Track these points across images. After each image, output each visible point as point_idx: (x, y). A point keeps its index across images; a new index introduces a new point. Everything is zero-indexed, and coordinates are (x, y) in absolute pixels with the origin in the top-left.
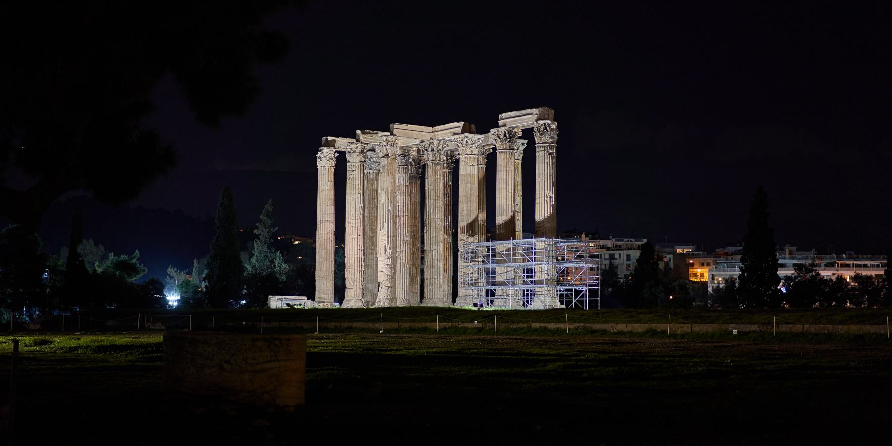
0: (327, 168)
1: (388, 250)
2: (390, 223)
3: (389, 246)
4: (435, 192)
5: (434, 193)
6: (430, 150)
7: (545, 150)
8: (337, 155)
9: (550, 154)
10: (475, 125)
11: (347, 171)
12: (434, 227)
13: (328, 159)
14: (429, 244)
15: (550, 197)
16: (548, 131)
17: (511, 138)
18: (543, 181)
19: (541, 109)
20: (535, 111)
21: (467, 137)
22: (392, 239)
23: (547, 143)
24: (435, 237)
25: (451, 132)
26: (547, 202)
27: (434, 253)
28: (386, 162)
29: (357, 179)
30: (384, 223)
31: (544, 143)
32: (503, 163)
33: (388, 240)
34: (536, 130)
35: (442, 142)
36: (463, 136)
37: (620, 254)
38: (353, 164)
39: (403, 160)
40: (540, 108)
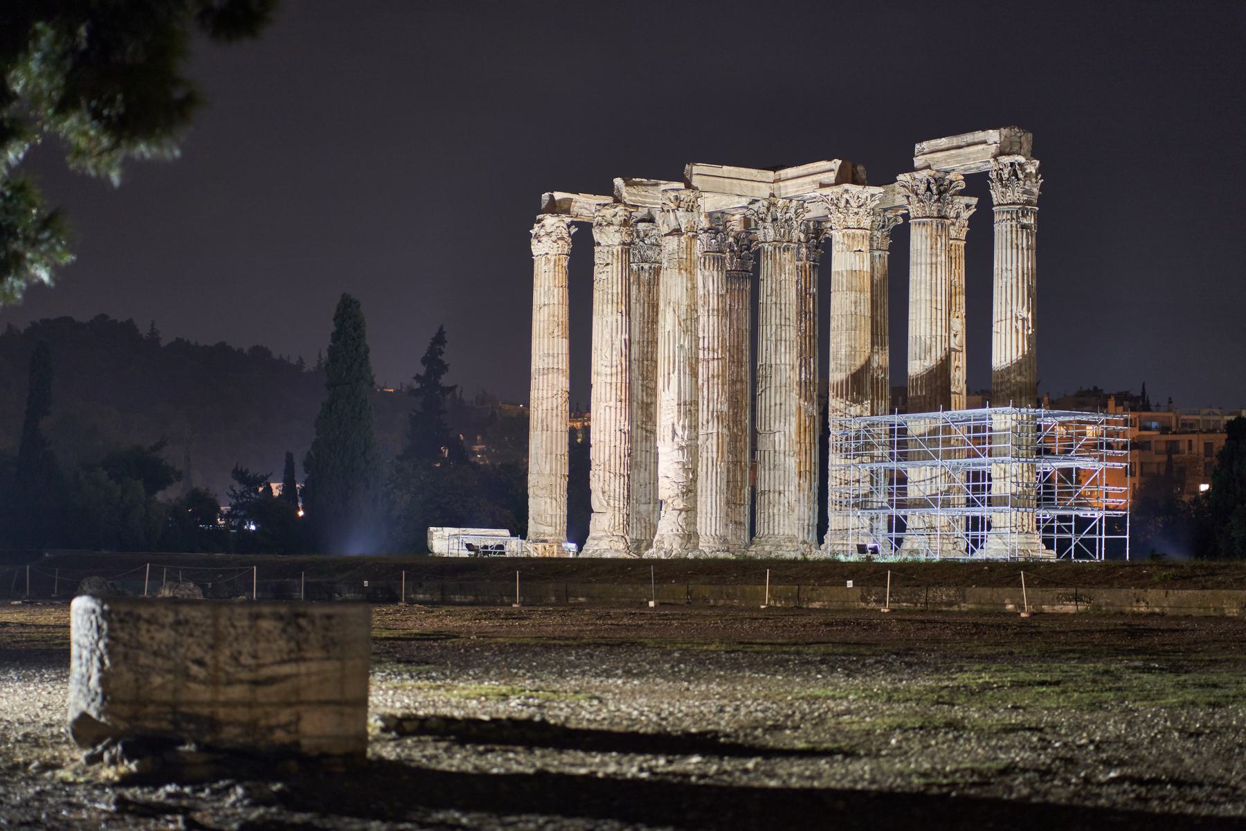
0: (553, 258)
1: (679, 431)
2: (685, 373)
3: (681, 423)
4: (781, 310)
5: (778, 311)
6: (769, 219)
7: (1013, 219)
8: (573, 230)
9: (1024, 227)
10: (864, 166)
11: (593, 264)
12: (778, 384)
13: (554, 238)
14: (768, 419)
15: (1023, 320)
16: (1019, 179)
17: (940, 193)
18: (1009, 285)
19: (1004, 131)
20: (993, 136)
21: (847, 191)
22: (689, 408)
23: (1018, 204)
24: (781, 404)
25: (814, 182)
26: (1017, 331)
27: (777, 439)
28: (676, 247)
29: (615, 281)
30: (672, 375)
31: (1010, 204)
32: (924, 247)
33: (679, 412)
34: (993, 175)
35: (794, 203)
36: (838, 189)
37: (1190, 442)
39: (713, 241)
40: (1002, 129)
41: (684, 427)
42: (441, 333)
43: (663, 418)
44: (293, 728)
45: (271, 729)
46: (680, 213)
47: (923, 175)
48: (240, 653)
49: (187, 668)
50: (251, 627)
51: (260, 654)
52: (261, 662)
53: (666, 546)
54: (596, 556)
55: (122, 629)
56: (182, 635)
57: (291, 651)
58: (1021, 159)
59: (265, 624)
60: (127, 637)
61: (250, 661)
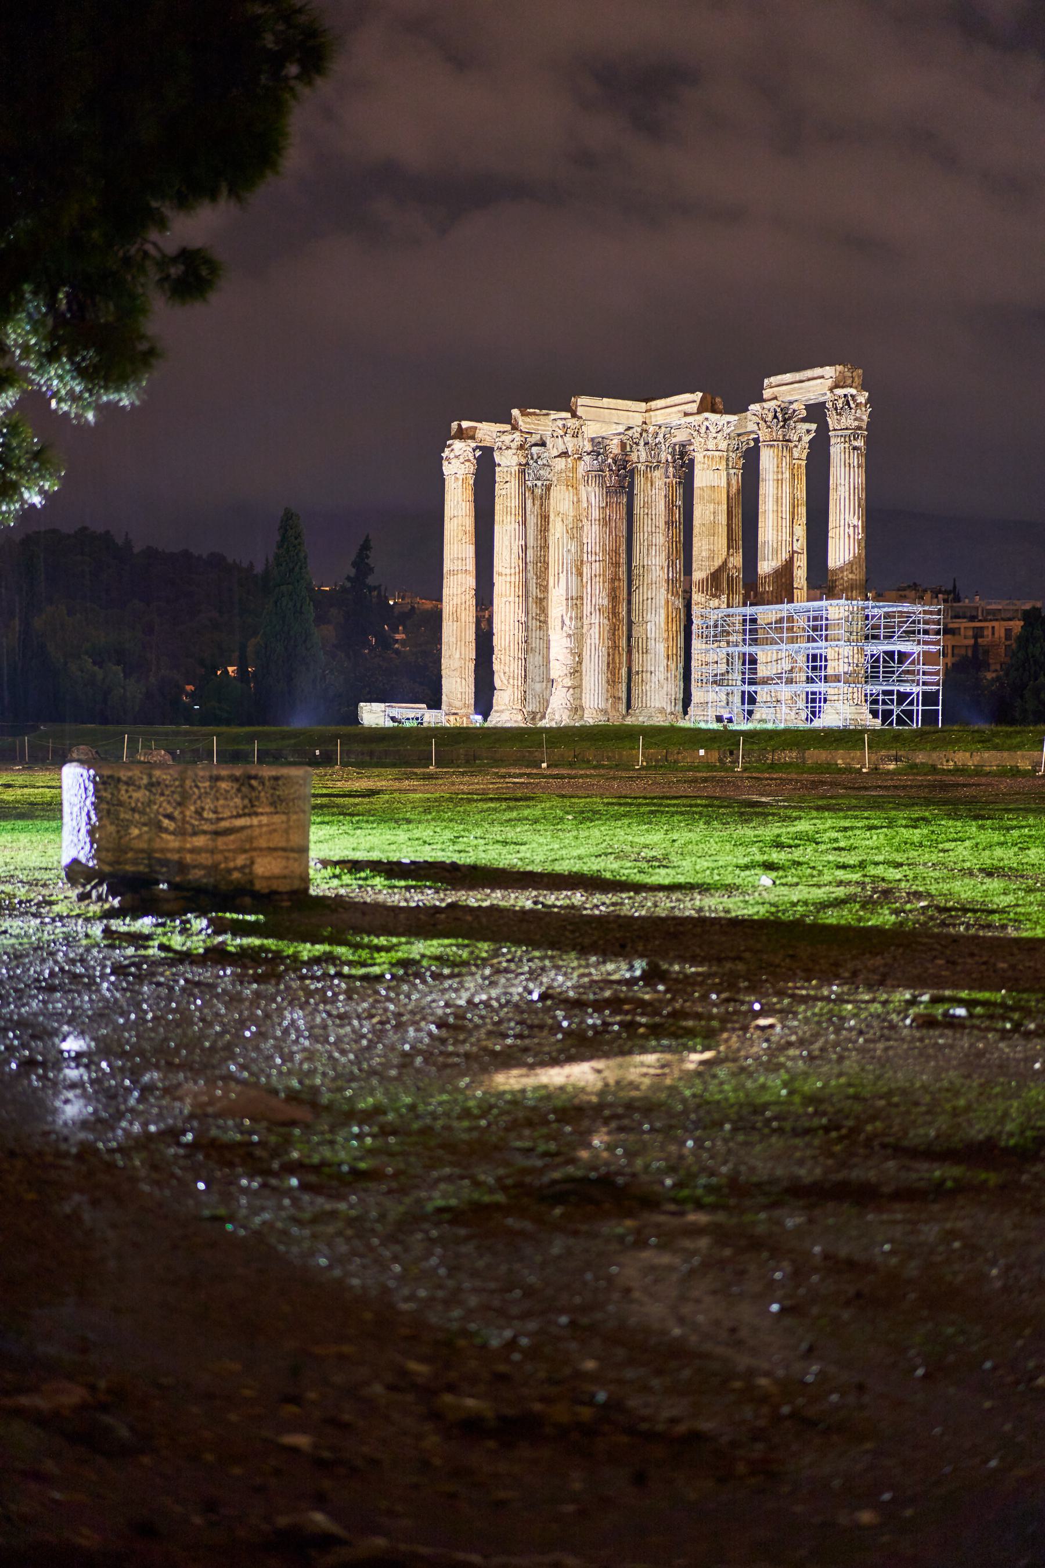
0: (461, 478)
1: (567, 622)
6: (642, 443)
8: (478, 453)
9: (855, 448)
13: (462, 460)
15: (854, 526)
17: (785, 420)
19: (839, 368)
20: (829, 371)
21: (707, 419)
22: (576, 601)
26: (849, 536)
27: (649, 628)
28: (563, 467)
34: (829, 405)
35: (663, 429)
36: (700, 418)
37: (993, 628)
38: (506, 469)
41: (571, 618)
42: (367, 540)
43: (554, 611)
44: (247, 871)
45: (229, 871)
46: (568, 438)
47: (772, 404)
48: (203, 809)
49: (160, 821)
50: (211, 788)
51: (220, 810)
52: (221, 816)
53: (557, 717)
54: (499, 725)
55: (105, 790)
56: (155, 794)
57: (245, 807)
58: (853, 391)
59: (224, 785)
60: (109, 796)
61: (212, 816)
